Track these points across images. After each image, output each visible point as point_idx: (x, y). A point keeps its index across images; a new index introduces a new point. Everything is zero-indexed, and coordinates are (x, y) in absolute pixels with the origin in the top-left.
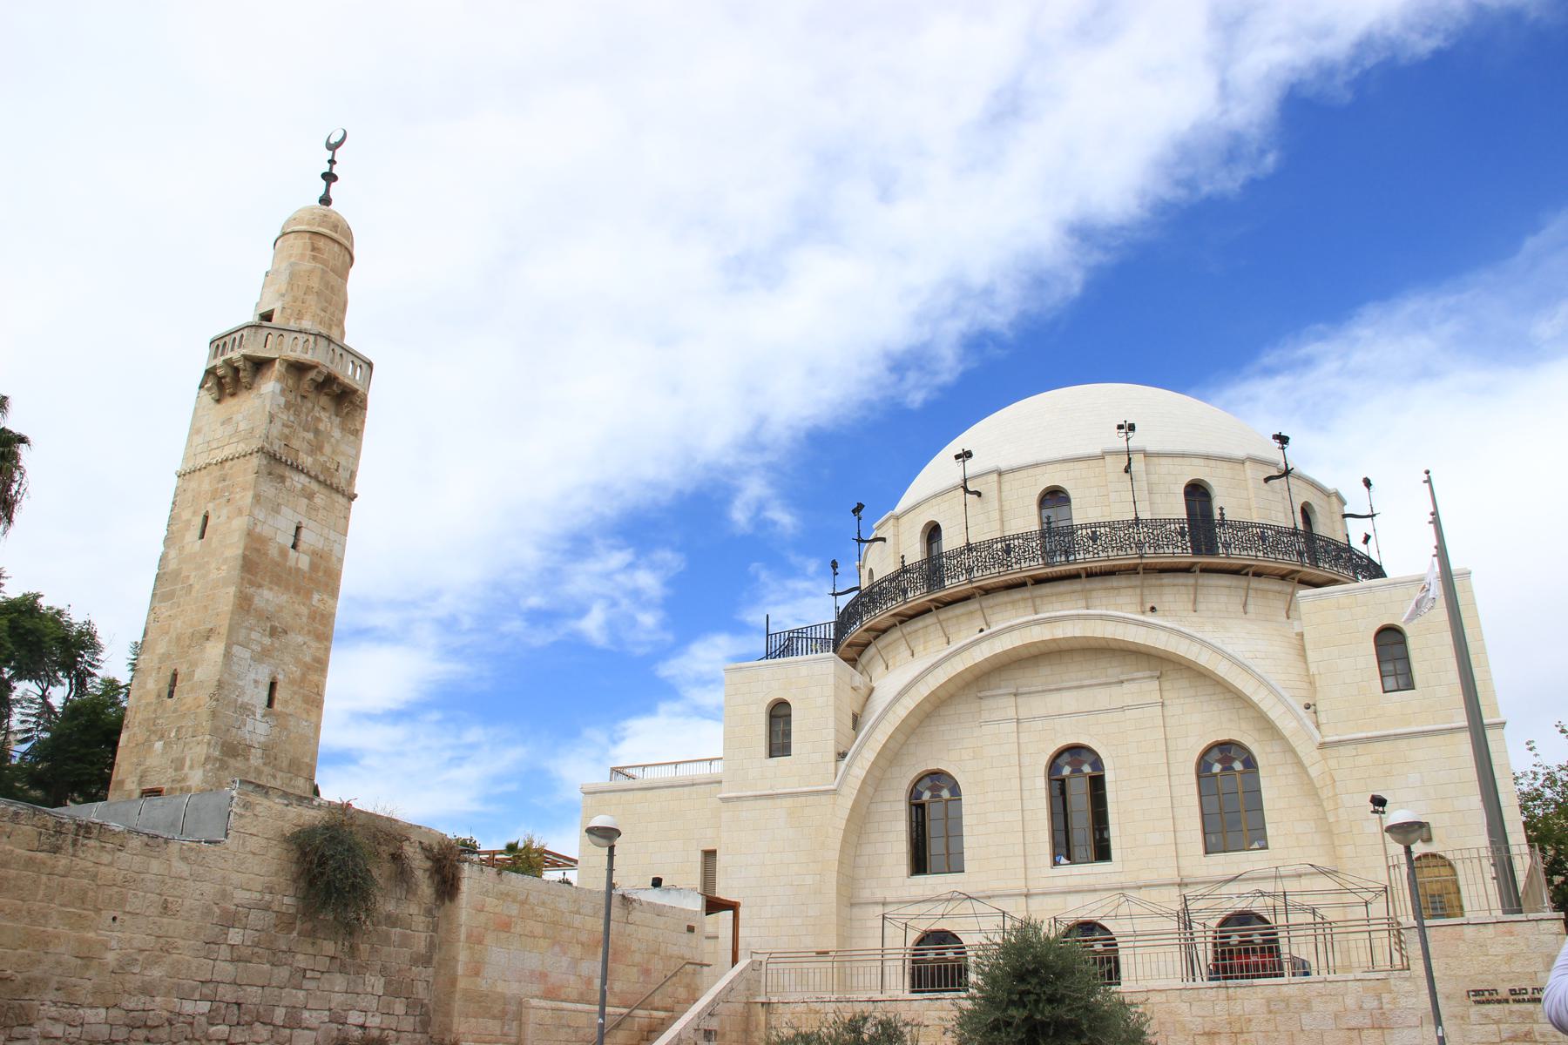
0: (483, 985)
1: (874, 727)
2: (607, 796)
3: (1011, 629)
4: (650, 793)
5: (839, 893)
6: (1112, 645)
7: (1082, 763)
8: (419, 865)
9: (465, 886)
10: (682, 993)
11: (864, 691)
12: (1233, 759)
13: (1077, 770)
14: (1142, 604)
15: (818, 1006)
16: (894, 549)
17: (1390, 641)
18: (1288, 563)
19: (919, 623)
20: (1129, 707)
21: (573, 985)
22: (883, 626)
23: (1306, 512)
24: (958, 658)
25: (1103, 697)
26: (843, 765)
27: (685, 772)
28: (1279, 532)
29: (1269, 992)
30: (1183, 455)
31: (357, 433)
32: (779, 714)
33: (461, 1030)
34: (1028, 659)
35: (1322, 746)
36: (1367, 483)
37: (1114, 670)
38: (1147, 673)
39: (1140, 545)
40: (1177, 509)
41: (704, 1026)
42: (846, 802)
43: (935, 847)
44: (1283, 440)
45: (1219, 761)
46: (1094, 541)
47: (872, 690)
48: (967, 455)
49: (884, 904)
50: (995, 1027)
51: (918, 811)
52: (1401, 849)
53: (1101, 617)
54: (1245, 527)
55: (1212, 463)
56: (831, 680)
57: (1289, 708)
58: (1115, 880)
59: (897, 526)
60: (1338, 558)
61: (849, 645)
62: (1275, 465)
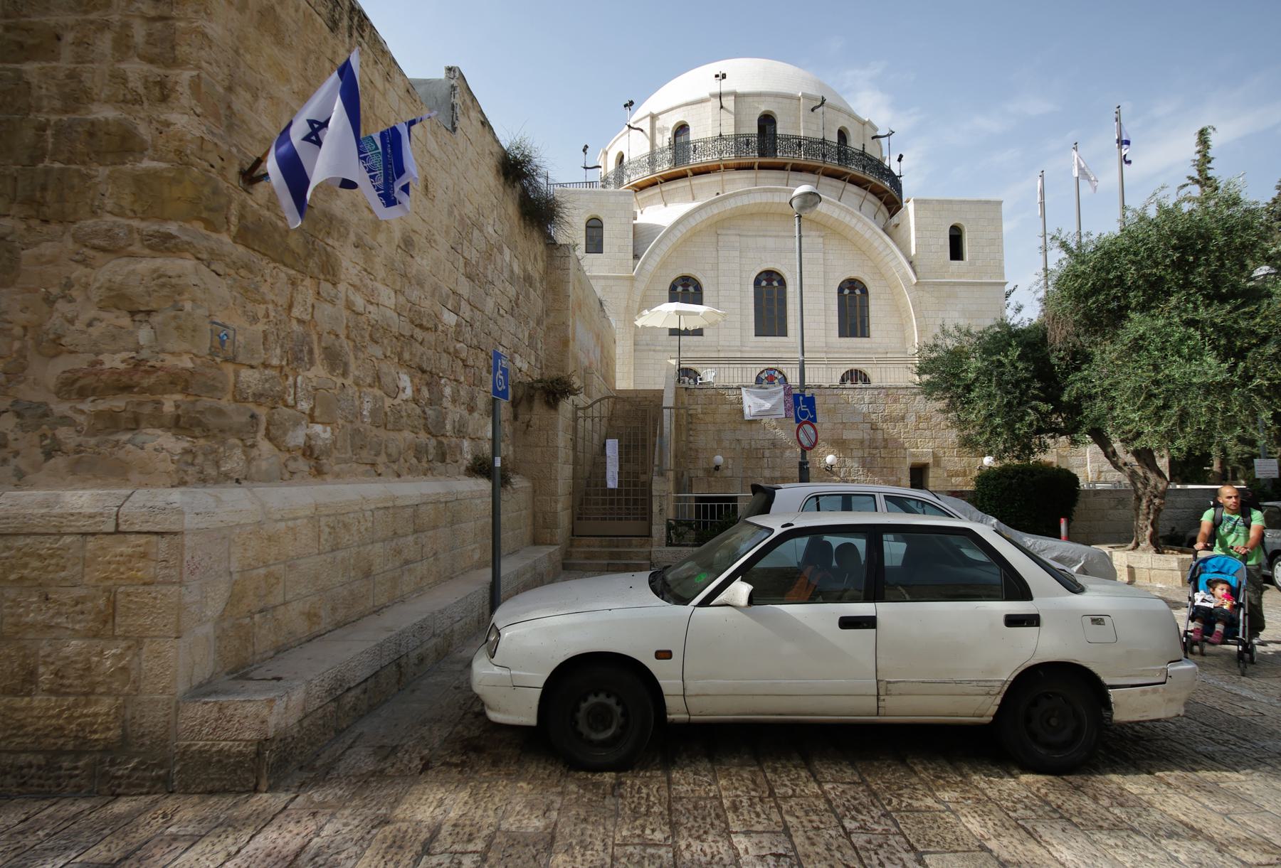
62: (876, 130)
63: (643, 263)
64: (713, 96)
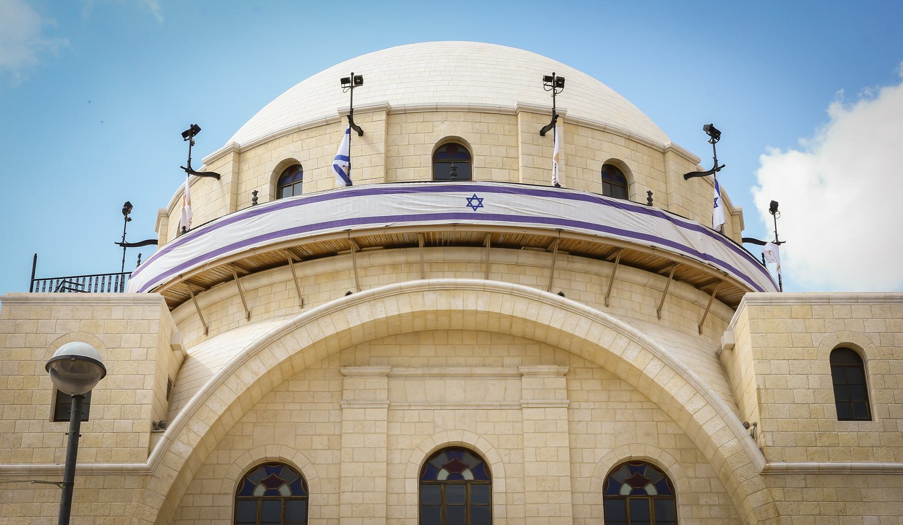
3: (400, 292)
7: (464, 467)
12: (646, 482)
22: (207, 280)
24: (327, 319)
25: (495, 390)
26: (162, 439)
30: (604, 130)
34: (406, 334)
36: (774, 207)
37: (511, 359)
38: (554, 368)
44: (714, 133)
45: (629, 482)
48: (359, 81)
53: (511, 293)
55: (632, 145)
62: (696, 162)
63: (170, 441)
64: (341, 114)
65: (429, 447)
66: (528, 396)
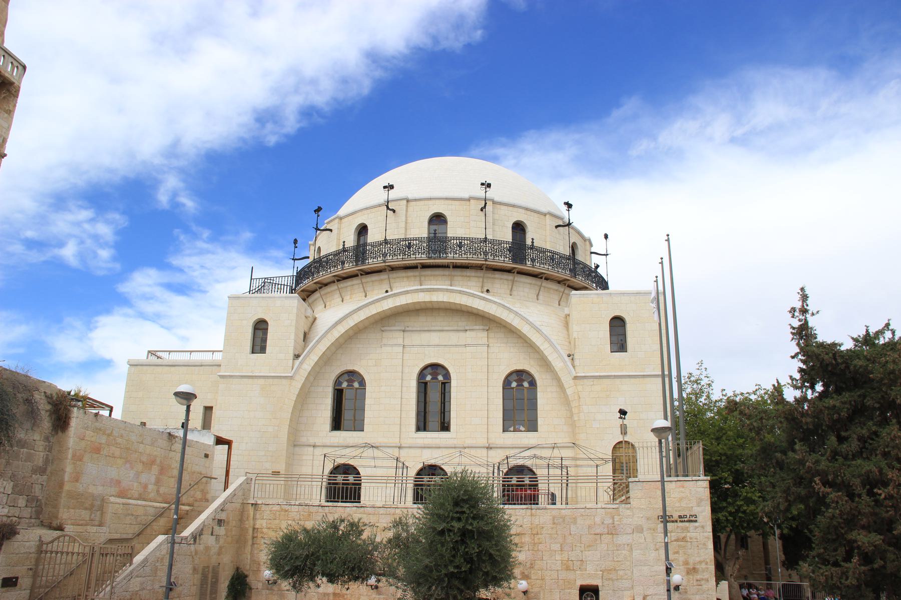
0: (80, 488)
1: (318, 342)
2: (145, 368)
3: (407, 292)
4: (173, 369)
5: (288, 438)
6: (463, 309)
7: (438, 374)
8: (44, 407)
9: (73, 423)
10: (199, 495)
11: (311, 320)
12: (524, 380)
13: (435, 378)
14: (482, 287)
15: (287, 507)
16: (336, 237)
17: (618, 324)
18: (565, 274)
19: (349, 283)
20: (469, 345)
21: (136, 488)
22: (325, 282)
23: (574, 247)
26: (297, 362)
27: (196, 357)
28: (562, 257)
29: (554, 513)
30: (514, 206)
31: (10, 113)
32: (261, 327)
33: (64, 517)
35: (576, 378)
36: (606, 237)
37: (462, 323)
38: (481, 327)
39: (486, 253)
40: (507, 236)
41: (218, 517)
42: (298, 384)
43: (347, 415)
44: (569, 206)
46: (460, 248)
47: (315, 319)
48: (392, 187)
49: (314, 446)
50: (442, 533)
51: (339, 395)
52: (657, 440)
53: (460, 292)
54: (543, 251)
55: (529, 213)
56: (295, 311)
57: (560, 355)
58: (451, 442)
59: (340, 223)
60: (589, 275)
61: (302, 291)
62: (562, 219)
65: (422, 365)
66: (469, 342)
